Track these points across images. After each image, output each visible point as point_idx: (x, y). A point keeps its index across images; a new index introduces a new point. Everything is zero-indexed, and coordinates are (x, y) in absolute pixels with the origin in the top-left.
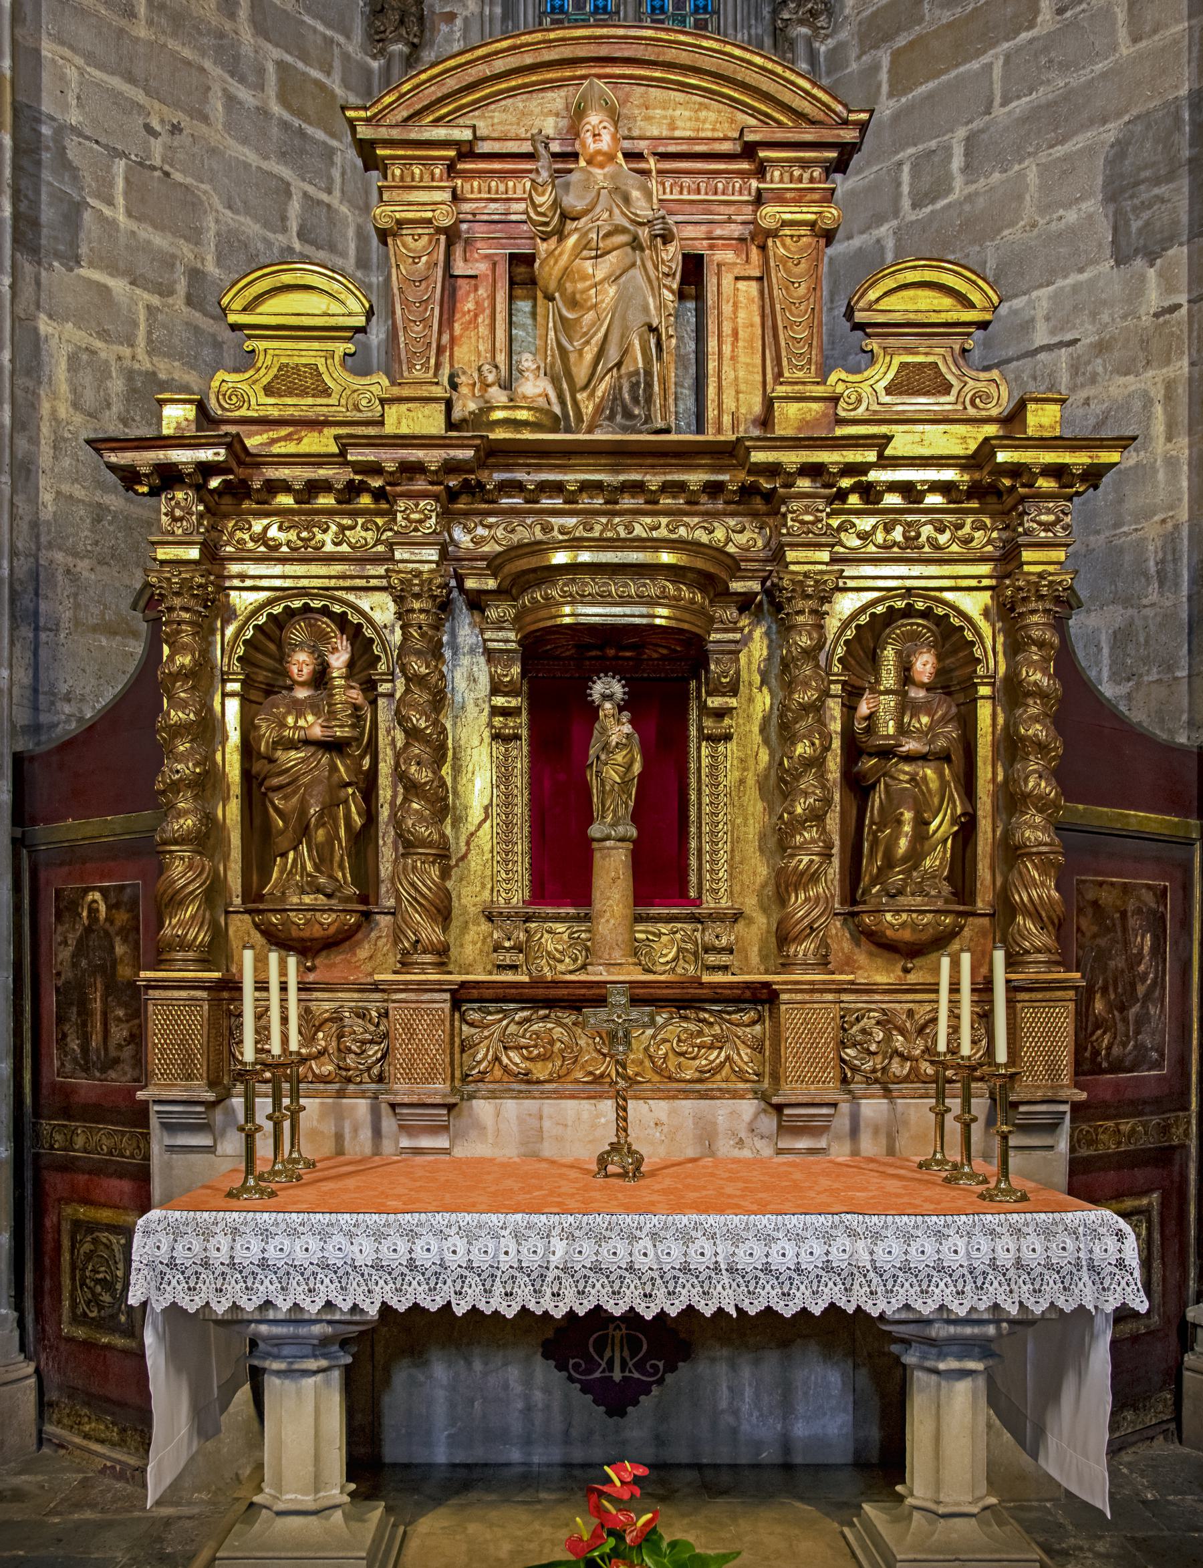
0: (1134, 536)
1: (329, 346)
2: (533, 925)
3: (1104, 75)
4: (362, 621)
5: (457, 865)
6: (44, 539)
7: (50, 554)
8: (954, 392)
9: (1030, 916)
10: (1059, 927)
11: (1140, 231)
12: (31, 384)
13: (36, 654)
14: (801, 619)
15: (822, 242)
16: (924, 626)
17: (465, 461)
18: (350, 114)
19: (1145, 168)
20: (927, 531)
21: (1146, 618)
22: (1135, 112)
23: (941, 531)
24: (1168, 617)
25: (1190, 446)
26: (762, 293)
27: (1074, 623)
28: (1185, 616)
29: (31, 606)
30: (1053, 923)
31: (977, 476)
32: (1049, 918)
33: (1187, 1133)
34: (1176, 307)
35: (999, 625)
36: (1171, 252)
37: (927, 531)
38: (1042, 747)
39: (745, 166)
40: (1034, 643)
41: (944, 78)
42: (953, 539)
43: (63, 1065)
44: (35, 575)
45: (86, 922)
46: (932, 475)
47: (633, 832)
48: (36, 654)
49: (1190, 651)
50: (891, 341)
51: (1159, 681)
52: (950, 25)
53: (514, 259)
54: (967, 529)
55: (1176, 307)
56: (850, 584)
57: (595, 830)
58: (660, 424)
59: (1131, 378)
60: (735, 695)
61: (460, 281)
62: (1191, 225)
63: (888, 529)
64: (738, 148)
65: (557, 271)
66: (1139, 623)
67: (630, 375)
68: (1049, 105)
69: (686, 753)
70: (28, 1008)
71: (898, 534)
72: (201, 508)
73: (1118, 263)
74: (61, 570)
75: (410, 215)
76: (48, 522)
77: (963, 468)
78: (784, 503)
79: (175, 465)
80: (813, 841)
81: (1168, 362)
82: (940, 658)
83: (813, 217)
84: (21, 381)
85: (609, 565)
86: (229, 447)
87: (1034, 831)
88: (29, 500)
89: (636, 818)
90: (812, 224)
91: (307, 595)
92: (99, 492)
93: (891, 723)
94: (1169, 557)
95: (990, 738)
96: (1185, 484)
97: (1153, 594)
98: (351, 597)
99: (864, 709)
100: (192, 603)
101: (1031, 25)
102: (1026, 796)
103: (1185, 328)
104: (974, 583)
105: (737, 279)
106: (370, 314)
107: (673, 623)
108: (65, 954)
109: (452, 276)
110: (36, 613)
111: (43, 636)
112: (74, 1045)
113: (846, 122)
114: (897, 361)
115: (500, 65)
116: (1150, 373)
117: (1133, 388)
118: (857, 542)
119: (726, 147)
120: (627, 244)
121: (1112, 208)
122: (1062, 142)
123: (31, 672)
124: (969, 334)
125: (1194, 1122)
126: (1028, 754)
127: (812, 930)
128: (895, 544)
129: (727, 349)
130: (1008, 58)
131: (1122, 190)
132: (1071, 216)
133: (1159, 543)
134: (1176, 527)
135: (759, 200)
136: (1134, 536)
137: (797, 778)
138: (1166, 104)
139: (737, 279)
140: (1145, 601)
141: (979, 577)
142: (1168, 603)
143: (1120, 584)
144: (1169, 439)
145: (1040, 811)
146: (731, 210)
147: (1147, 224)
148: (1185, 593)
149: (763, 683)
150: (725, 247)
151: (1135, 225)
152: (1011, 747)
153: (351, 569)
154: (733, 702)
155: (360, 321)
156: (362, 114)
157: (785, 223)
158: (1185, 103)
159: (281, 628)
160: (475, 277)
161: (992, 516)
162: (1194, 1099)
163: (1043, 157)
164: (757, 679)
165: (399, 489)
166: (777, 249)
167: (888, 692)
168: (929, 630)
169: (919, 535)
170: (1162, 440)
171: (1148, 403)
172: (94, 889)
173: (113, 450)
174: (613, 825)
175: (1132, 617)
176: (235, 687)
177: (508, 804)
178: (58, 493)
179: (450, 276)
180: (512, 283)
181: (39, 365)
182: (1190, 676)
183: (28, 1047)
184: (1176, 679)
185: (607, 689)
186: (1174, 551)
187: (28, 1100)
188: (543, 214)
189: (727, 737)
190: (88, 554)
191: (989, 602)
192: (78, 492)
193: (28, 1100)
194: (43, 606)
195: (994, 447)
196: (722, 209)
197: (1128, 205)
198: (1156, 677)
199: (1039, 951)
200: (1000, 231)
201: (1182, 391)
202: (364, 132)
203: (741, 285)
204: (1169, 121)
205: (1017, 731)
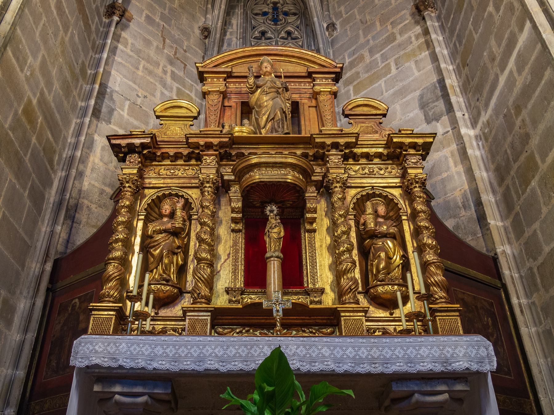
0: (452, 196)
1: (186, 122)
2: (244, 296)
3: (412, 81)
4: (189, 197)
5: (216, 274)
6: (82, 196)
7: (83, 200)
8: (379, 133)
9: (435, 286)
10: (447, 290)
11: (432, 115)
12: (88, 151)
13: (71, 230)
14: (336, 189)
15: (333, 96)
16: (380, 201)
17: (226, 142)
18: (197, 65)
19: (430, 99)
20: (376, 170)
21: (462, 220)
22: (423, 87)
23: (381, 169)
24: (470, 219)
25: (463, 167)
26: (317, 110)
27: (428, 187)
28: (475, 217)
29: (73, 214)
30: (444, 288)
31: (389, 151)
32: (442, 285)
33: (531, 408)
34: (448, 131)
35: (405, 197)
36: (443, 118)
37: (376, 170)
38: (427, 228)
39: (309, 80)
40: (418, 197)
41: (369, 89)
42: (385, 171)
43: (47, 374)
44: (76, 206)
45: (70, 312)
46: (374, 150)
47: (281, 255)
48: (71, 230)
49: (480, 228)
50: (357, 120)
51: (472, 239)
52: (368, 77)
53: (243, 103)
54: (389, 169)
55: (448, 131)
56: (353, 185)
57: (268, 255)
58: (286, 131)
59: (439, 153)
60: (316, 213)
61: (226, 108)
62: (446, 110)
63: (363, 169)
64: (307, 75)
65: (255, 100)
66: (460, 222)
67: (277, 121)
68: (399, 90)
69: (301, 237)
70: (37, 354)
71: (366, 171)
72: (139, 160)
73: (428, 124)
74: (85, 206)
75: (213, 89)
76: (85, 191)
77: (385, 148)
78: (328, 157)
79: (133, 144)
80: (347, 258)
81: (449, 146)
82: (387, 208)
83: (329, 90)
84: (85, 150)
85: (272, 167)
86: (152, 138)
87: (430, 257)
88: (80, 183)
89: (282, 251)
90: (330, 92)
91: (171, 189)
92: (103, 186)
93: (372, 224)
94: (465, 200)
95: (409, 233)
96: (464, 178)
97: (463, 212)
98: (185, 190)
99: (362, 221)
100: (132, 186)
101: (390, 73)
102: (425, 244)
103: (452, 136)
104: (394, 185)
105: (309, 107)
106: (199, 113)
107: (292, 181)
108: (58, 327)
109: (224, 106)
110: (74, 217)
111: (75, 225)
112: (54, 364)
113: (336, 67)
114: (359, 125)
115: (239, 55)
116: (445, 150)
117: (440, 155)
118: (354, 173)
119: (304, 74)
120: (275, 92)
121: (422, 111)
122: (405, 97)
123: (68, 235)
124: (381, 118)
125: (533, 405)
126: (422, 231)
127: (351, 290)
128: (366, 173)
129: (307, 123)
130: (385, 82)
131: (424, 106)
132: (411, 115)
133: (461, 197)
134: (465, 191)
135: (314, 86)
136: (452, 196)
137: (340, 238)
138: (431, 84)
139: (309, 107)
140: (461, 215)
141: (396, 183)
142: (469, 214)
143: (451, 212)
144: (456, 167)
145: (431, 249)
146: (306, 90)
147: (434, 112)
148: (474, 210)
149: (326, 214)
150: (305, 99)
151: (430, 114)
152: (417, 233)
153: (186, 181)
154: (315, 215)
155: (196, 115)
156: (201, 65)
157: (321, 91)
158: (437, 83)
159: (161, 202)
160: (231, 106)
161: (397, 165)
162: (531, 394)
163: (400, 102)
164: (324, 213)
165: (204, 153)
166: (321, 98)
167: (369, 214)
168: (382, 202)
169: (373, 171)
170: (453, 167)
171: (446, 158)
172: (76, 298)
173: (114, 139)
174: (274, 252)
175: (458, 221)
176: (143, 217)
177: (237, 252)
178: (90, 183)
179: (223, 106)
180: (242, 113)
181: (92, 147)
182: (483, 235)
183: (33, 371)
184: (478, 237)
185: (271, 210)
186: (466, 198)
187: (28, 394)
188: (251, 85)
189: (314, 231)
190: (96, 203)
191: (401, 192)
192: (96, 184)
193: (28, 394)
194: (77, 215)
195: (392, 137)
196: (303, 90)
197: (427, 109)
198: (471, 238)
199: (441, 298)
200: (391, 122)
201: (456, 154)
202: (200, 69)
203: (311, 109)
204: (433, 88)
205: (417, 225)
